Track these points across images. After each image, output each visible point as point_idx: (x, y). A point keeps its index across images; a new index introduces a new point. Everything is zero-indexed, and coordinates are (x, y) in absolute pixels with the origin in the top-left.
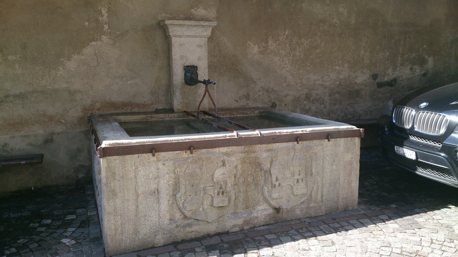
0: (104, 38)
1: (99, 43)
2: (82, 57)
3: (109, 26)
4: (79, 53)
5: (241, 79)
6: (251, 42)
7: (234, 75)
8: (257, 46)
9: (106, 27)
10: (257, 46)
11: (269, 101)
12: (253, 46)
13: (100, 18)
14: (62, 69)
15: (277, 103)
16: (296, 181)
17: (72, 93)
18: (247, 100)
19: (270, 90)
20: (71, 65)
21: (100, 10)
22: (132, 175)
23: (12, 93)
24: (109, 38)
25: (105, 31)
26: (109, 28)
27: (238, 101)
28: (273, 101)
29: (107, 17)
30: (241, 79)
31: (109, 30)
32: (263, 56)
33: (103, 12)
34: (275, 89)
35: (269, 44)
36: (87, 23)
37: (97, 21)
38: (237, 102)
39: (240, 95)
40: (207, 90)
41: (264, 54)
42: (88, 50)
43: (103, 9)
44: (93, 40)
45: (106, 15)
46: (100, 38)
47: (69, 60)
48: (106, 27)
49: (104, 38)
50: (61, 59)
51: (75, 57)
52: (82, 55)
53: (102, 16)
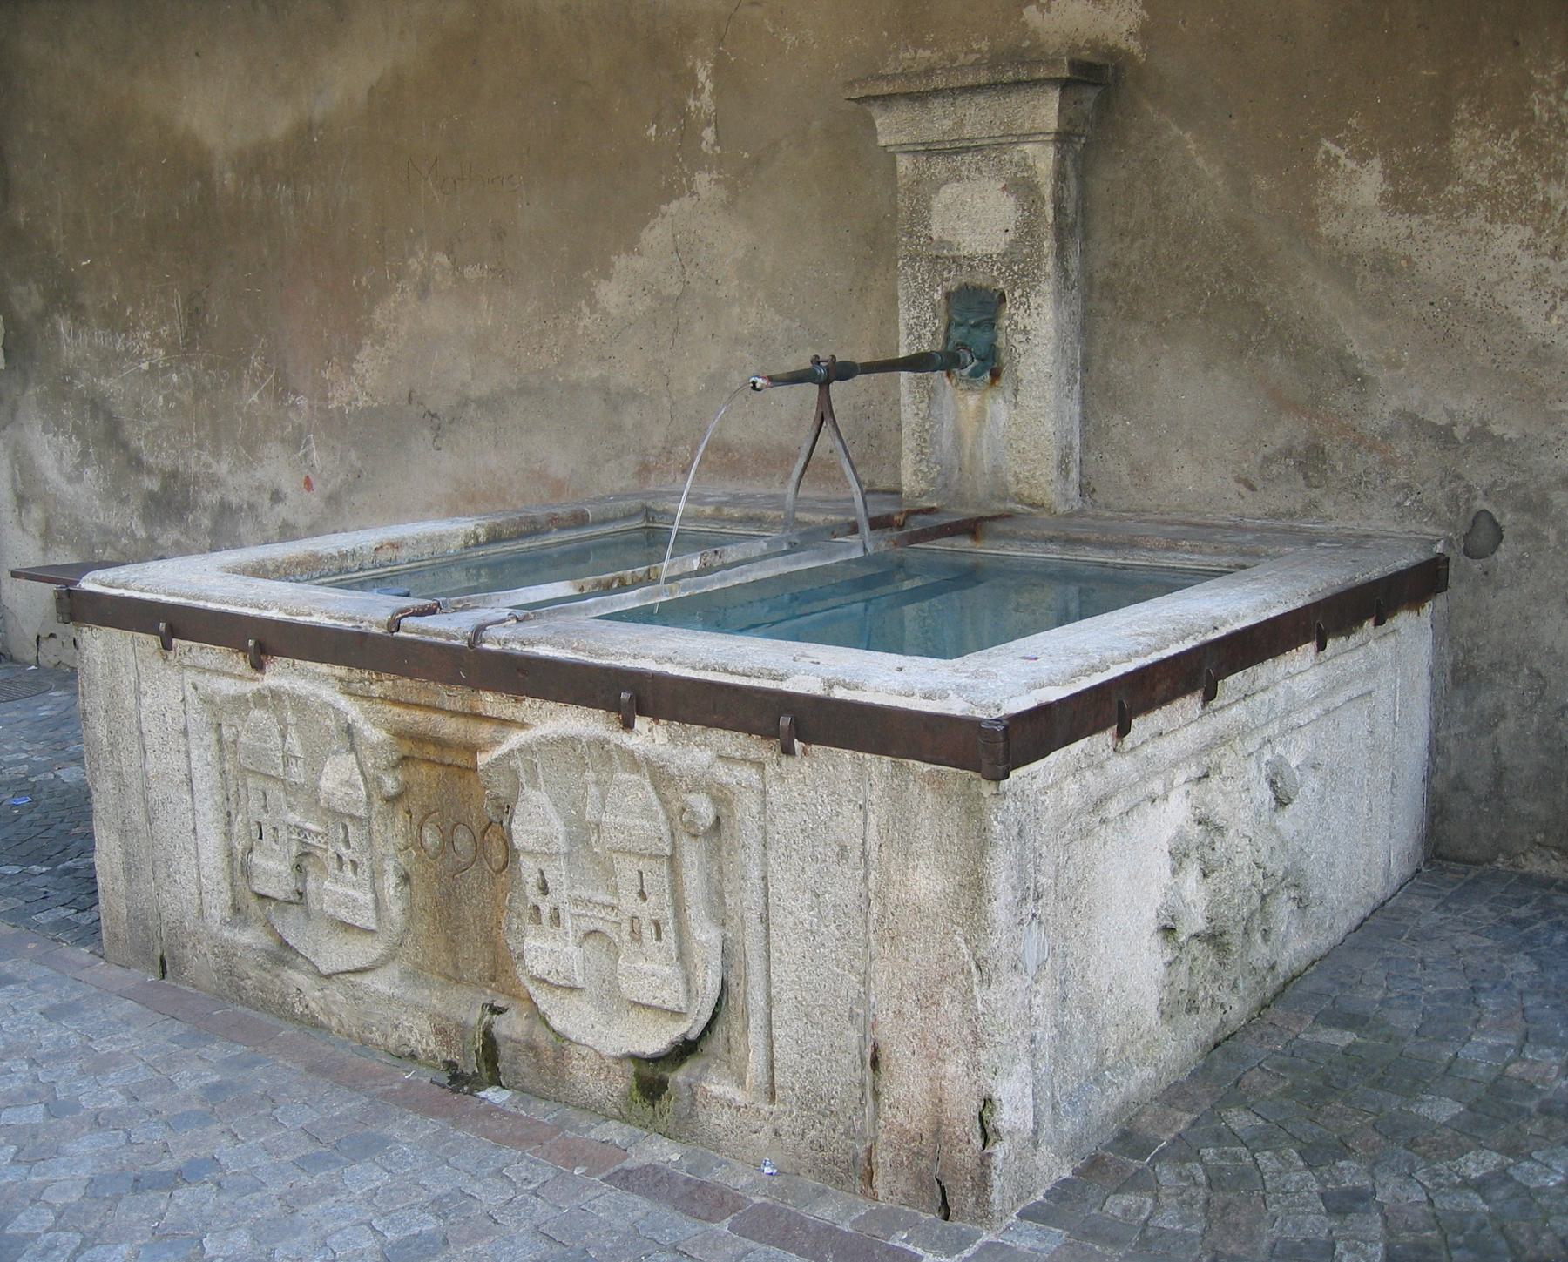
0: (703, 180)
1: (686, 203)
2: (639, 263)
3: (717, 133)
4: (629, 249)
5: (1276, 359)
6: (1339, 143)
7: (1233, 335)
8: (1376, 163)
9: (709, 134)
10: (1376, 163)
11: (1453, 498)
12: (1351, 165)
13: (691, 103)
14: (586, 310)
15: (1507, 519)
16: (626, 927)
17: (615, 399)
18: (1309, 486)
19: (1460, 433)
20: (610, 294)
21: (693, 69)
22: (130, 702)
23: (474, 393)
24: (718, 181)
25: (706, 154)
26: (717, 143)
27: (1259, 484)
28: (1480, 504)
29: (712, 95)
30: (1276, 359)
31: (718, 149)
32: (1415, 222)
33: (702, 76)
34: (1497, 430)
35: (1460, 144)
36: (652, 131)
37: (682, 112)
38: (1252, 488)
39: (1268, 450)
40: (825, 414)
41: (1423, 210)
42: (656, 235)
43: (699, 64)
44: (670, 194)
45: (709, 86)
46: (691, 182)
47: (608, 277)
48: (709, 134)
49: (703, 180)
50: (585, 275)
51: (621, 262)
52: (640, 254)
53: (697, 94)
